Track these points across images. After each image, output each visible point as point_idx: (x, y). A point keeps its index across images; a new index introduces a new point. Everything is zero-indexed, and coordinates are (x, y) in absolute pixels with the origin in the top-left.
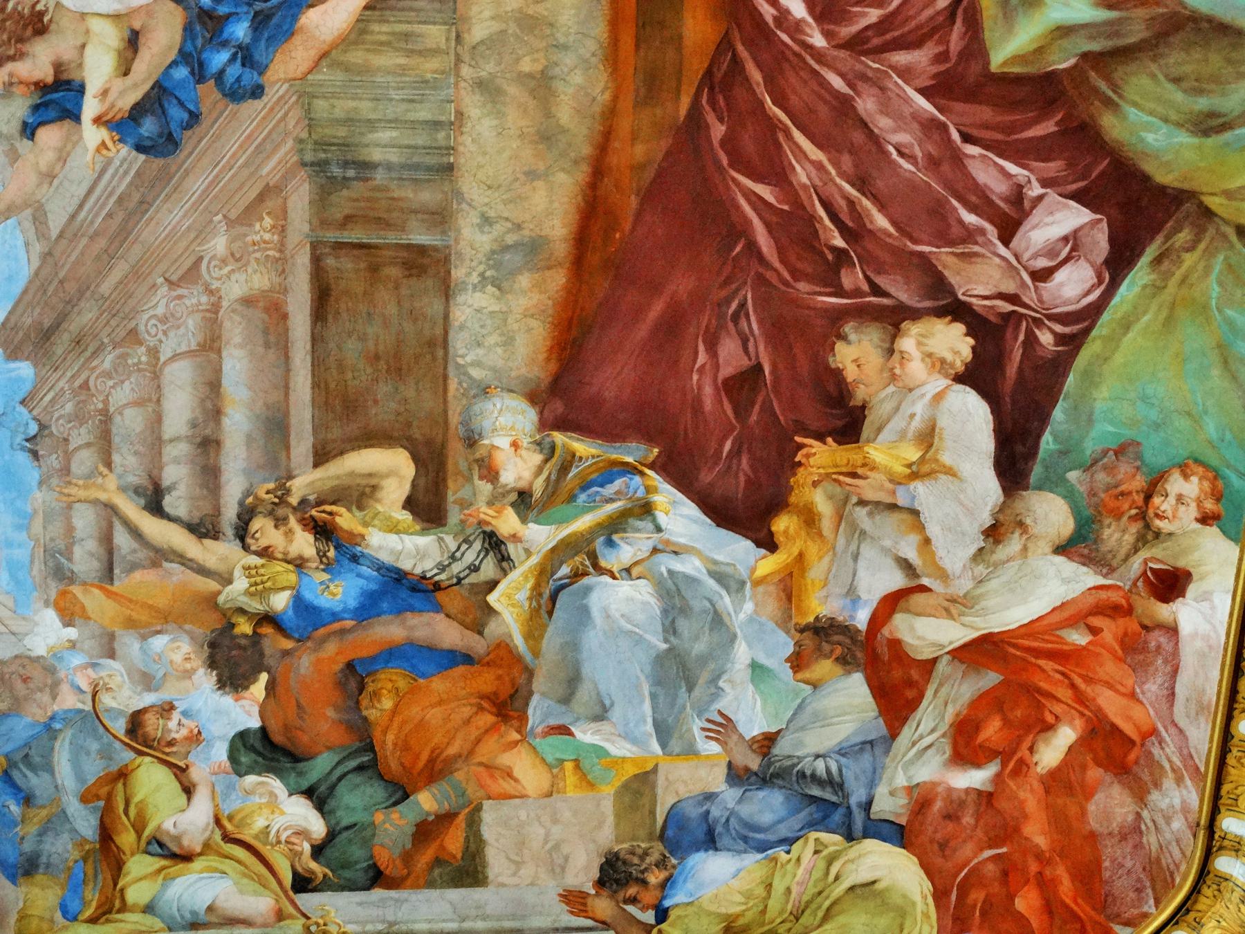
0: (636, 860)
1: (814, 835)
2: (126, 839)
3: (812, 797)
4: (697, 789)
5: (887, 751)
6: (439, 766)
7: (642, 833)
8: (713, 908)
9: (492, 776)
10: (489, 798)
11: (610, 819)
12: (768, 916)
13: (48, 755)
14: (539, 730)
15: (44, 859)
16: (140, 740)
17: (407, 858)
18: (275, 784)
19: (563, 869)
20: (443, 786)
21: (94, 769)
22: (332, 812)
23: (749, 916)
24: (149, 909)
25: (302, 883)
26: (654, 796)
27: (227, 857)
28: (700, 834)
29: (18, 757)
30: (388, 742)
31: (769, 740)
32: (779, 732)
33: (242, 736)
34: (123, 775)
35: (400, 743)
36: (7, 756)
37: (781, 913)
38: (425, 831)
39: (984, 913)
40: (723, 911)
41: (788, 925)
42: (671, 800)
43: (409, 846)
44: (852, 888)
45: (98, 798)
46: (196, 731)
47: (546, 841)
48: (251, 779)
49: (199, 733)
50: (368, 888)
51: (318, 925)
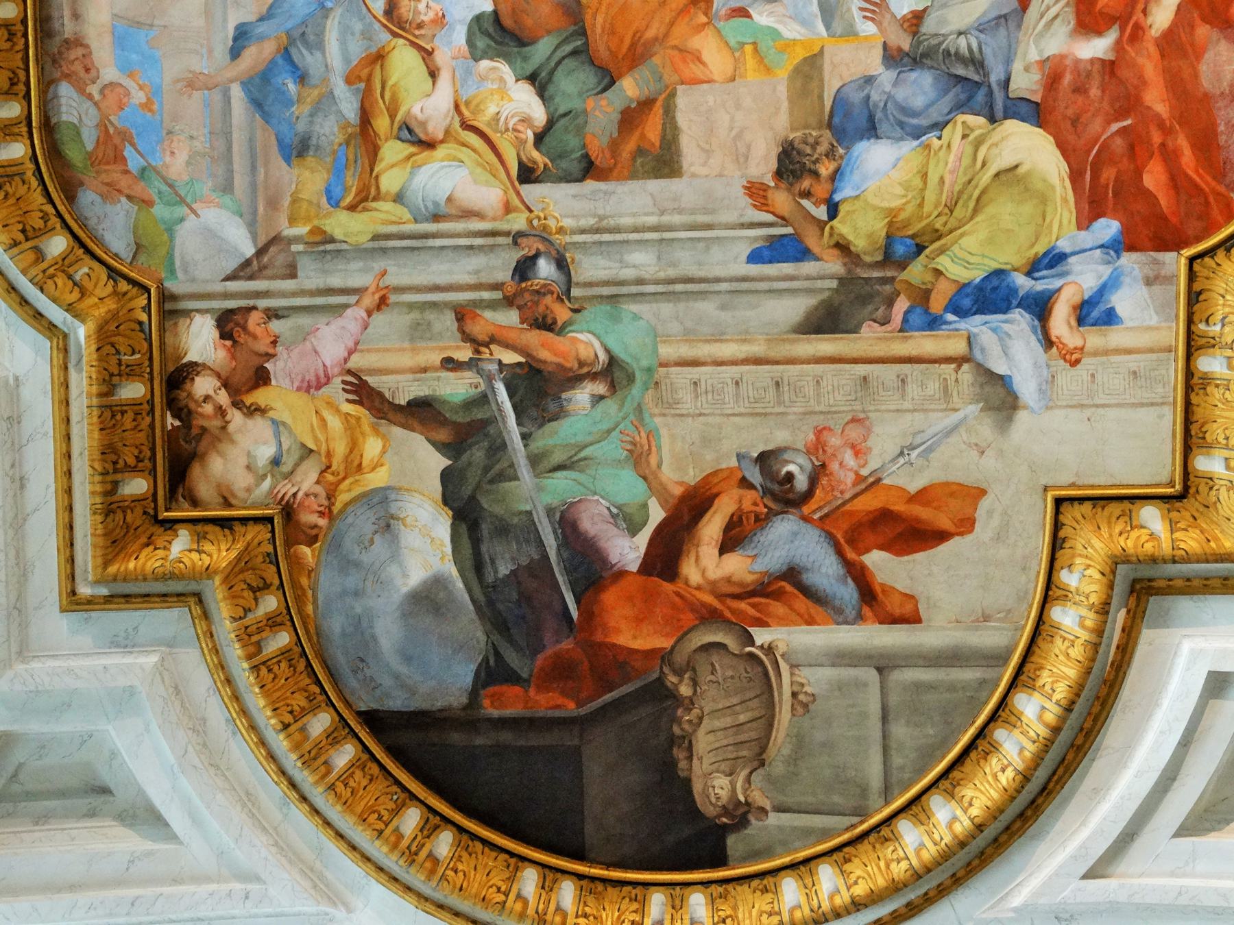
0: (808, 150)
1: (961, 118)
2: (382, 124)
3: (957, 76)
4: (857, 71)
5: (1019, 26)
6: (640, 50)
7: (813, 121)
8: (876, 201)
9: (684, 61)
10: (682, 83)
11: (785, 105)
12: (926, 209)
13: (320, 35)
14: (723, 12)
15: (314, 141)
16: (396, 21)
17: (614, 146)
18: (505, 69)
19: (747, 158)
20: (644, 72)
21: (357, 50)
22: (552, 98)
23: (910, 209)
24: (399, 198)
25: (527, 174)
26: (822, 81)
27: (464, 145)
28: (863, 122)
29: (296, 34)
30: (597, 23)
31: (917, 17)
32: (925, 10)
33: (478, 19)
34: (379, 57)
35: (608, 26)
36: (288, 33)
37: (936, 207)
38: (630, 118)
39: (1115, 194)
40: (886, 204)
41: (943, 219)
42: (836, 84)
43: (615, 135)
44: (997, 175)
45: (360, 79)
46: (440, 14)
47: (731, 129)
48: (485, 64)
49: (444, 16)
50: (580, 180)
51: (539, 218)
